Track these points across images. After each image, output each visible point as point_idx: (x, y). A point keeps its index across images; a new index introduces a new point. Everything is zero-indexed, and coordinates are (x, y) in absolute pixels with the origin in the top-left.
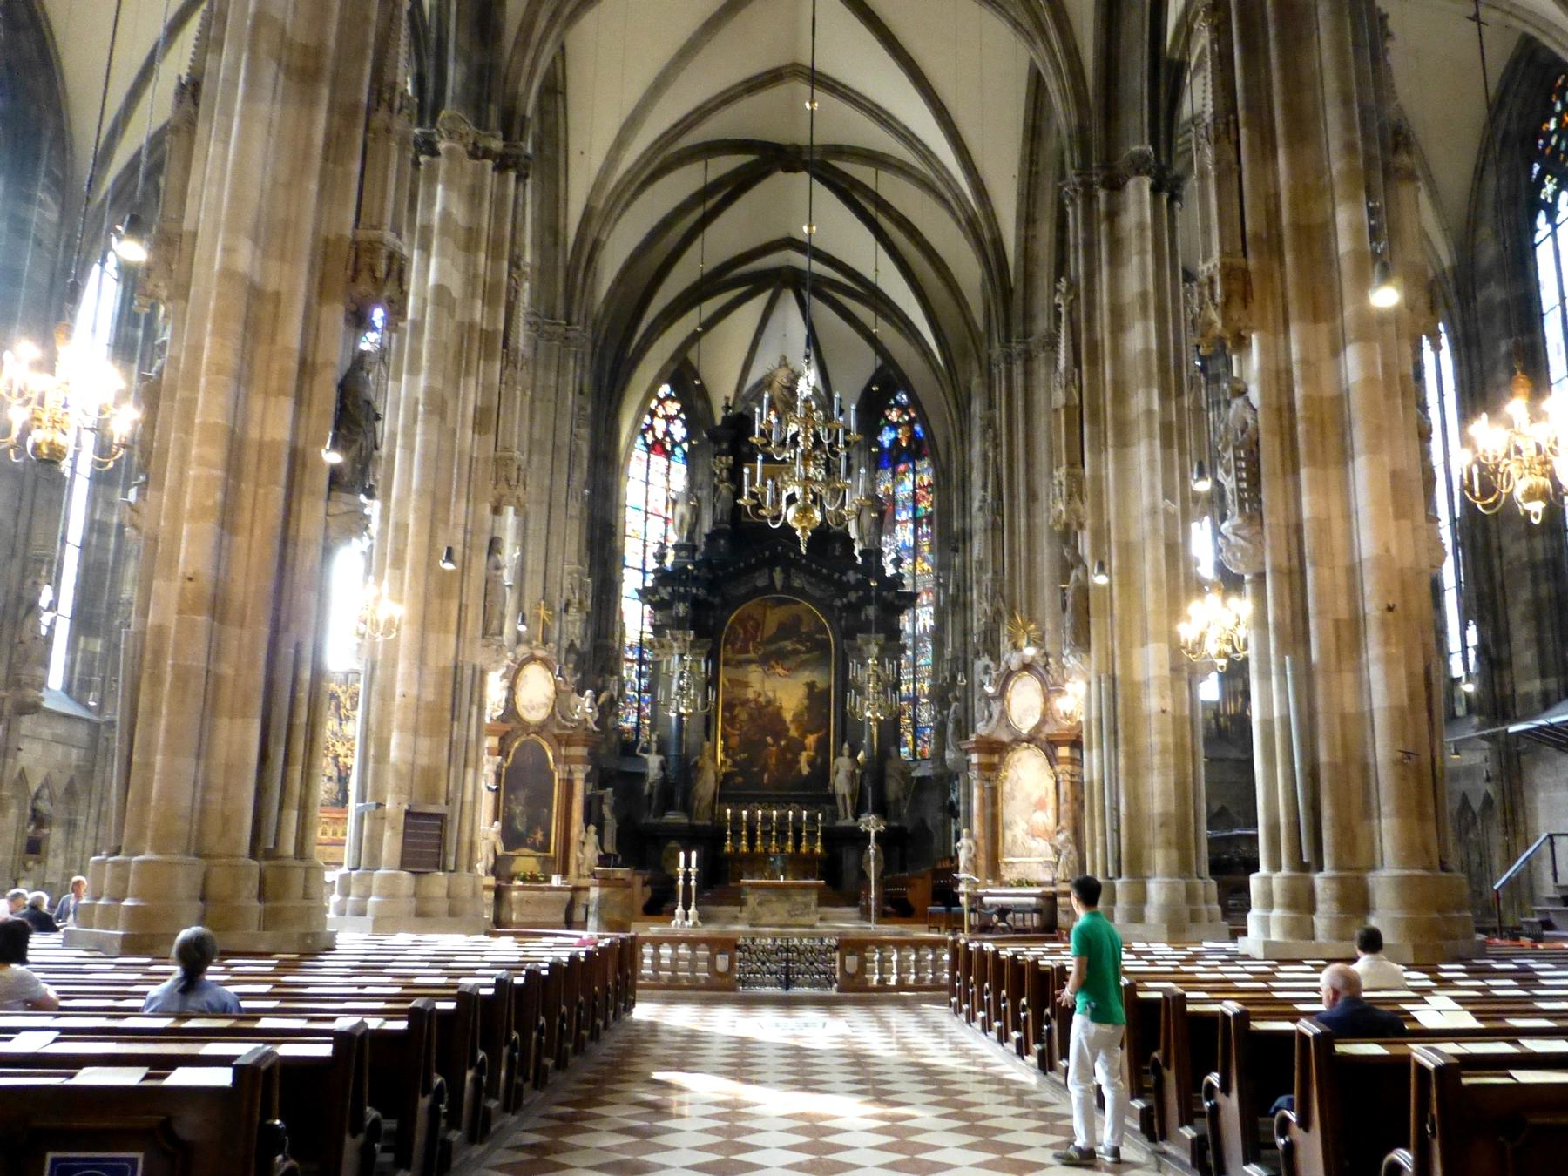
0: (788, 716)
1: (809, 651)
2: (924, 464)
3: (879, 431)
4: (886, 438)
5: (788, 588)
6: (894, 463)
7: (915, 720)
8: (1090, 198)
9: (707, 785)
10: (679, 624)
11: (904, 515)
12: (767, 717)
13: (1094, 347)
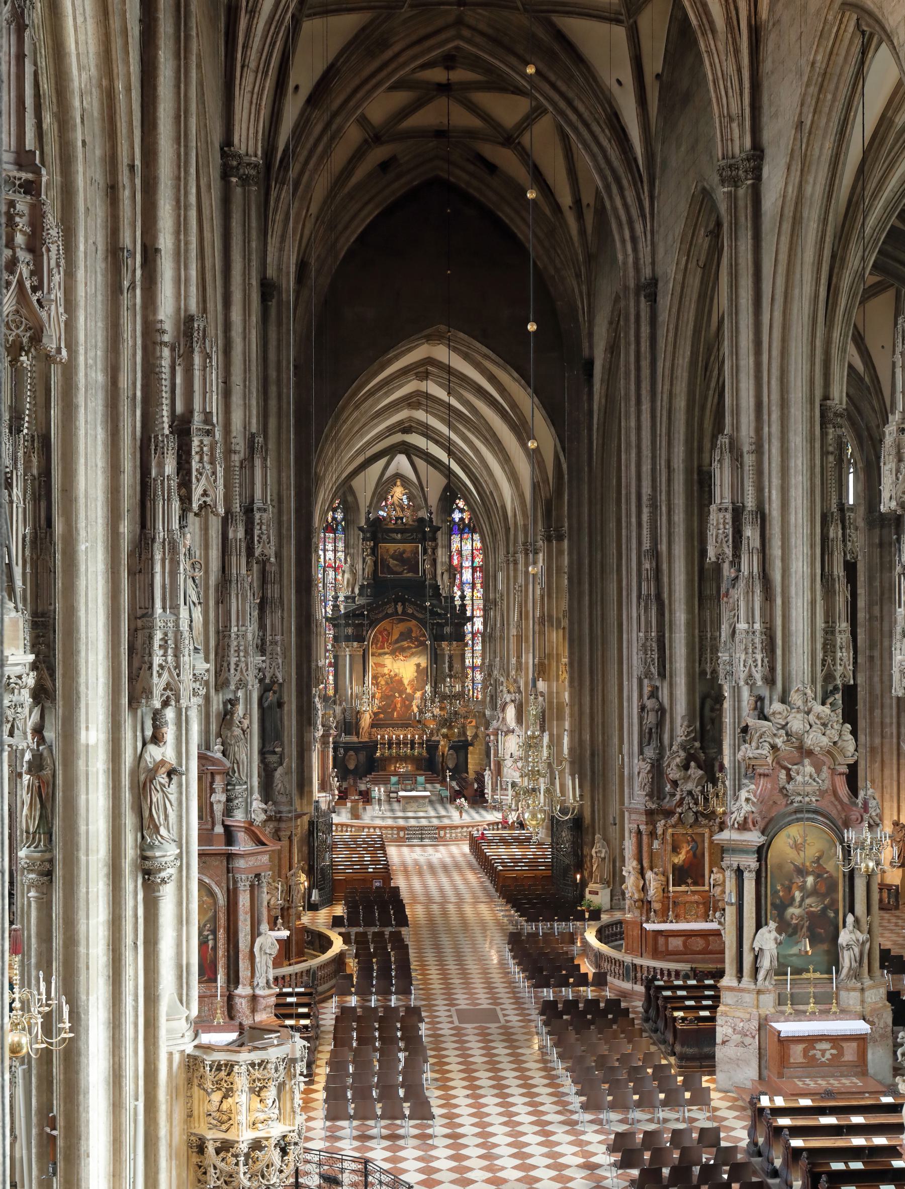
0: (406, 682)
1: (417, 647)
2: (476, 537)
3: (453, 511)
4: (457, 516)
5: (404, 613)
6: (462, 532)
7: (473, 680)
8: (527, 554)
9: (366, 720)
10: (348, 639)
11: (467, 564)
12: (395, 683)
13: (527, 613)
